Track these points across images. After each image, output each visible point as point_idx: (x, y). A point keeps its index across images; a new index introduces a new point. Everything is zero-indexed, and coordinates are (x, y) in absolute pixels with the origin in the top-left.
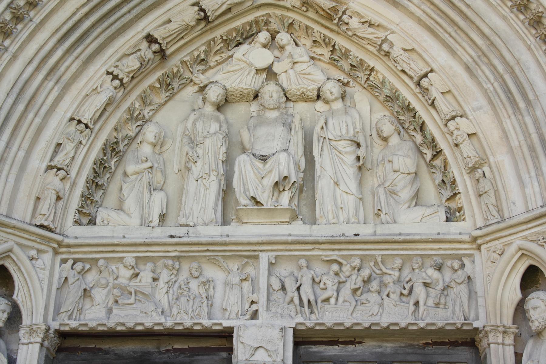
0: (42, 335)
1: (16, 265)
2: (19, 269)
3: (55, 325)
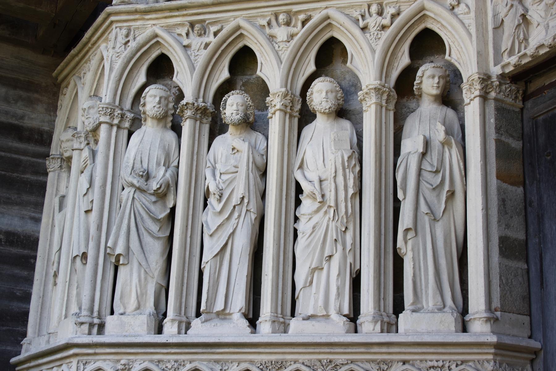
0: (478, 87)
1: (438, 22)
2: (442, 25)
3: (496, 71)
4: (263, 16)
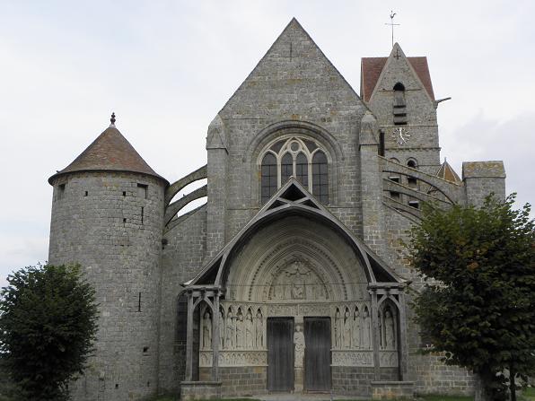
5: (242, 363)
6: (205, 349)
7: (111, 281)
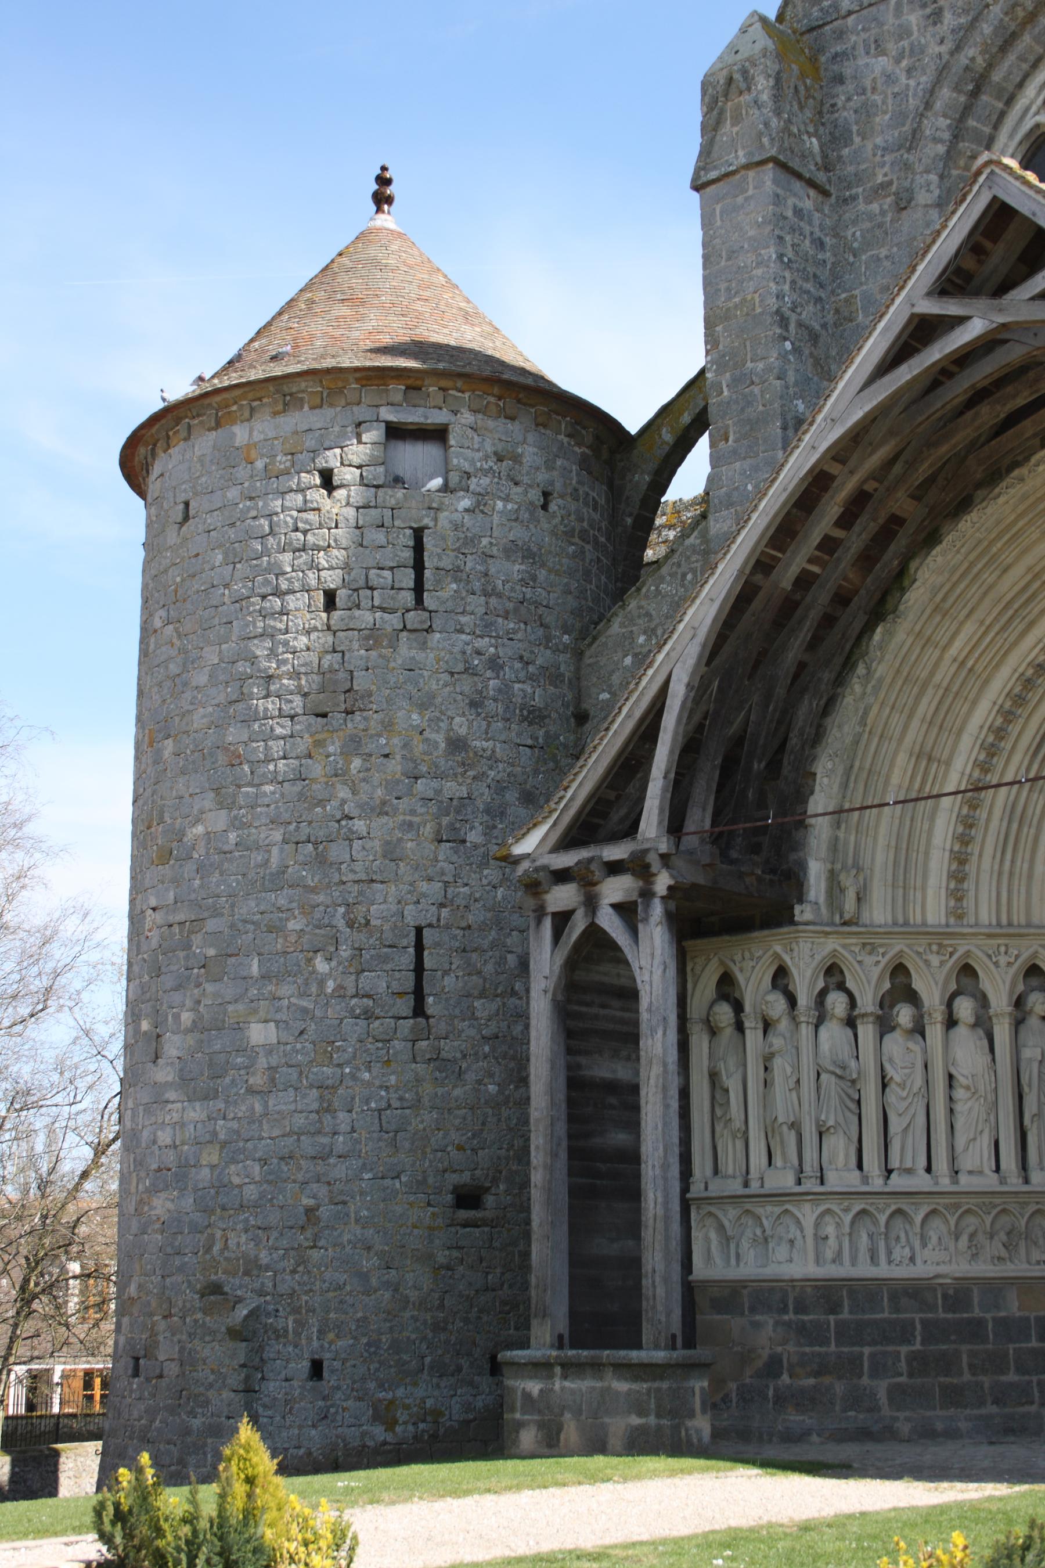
4: (920, 945)
5: (934, 1258)
6: (716, 1188)
7: (277, 880)
